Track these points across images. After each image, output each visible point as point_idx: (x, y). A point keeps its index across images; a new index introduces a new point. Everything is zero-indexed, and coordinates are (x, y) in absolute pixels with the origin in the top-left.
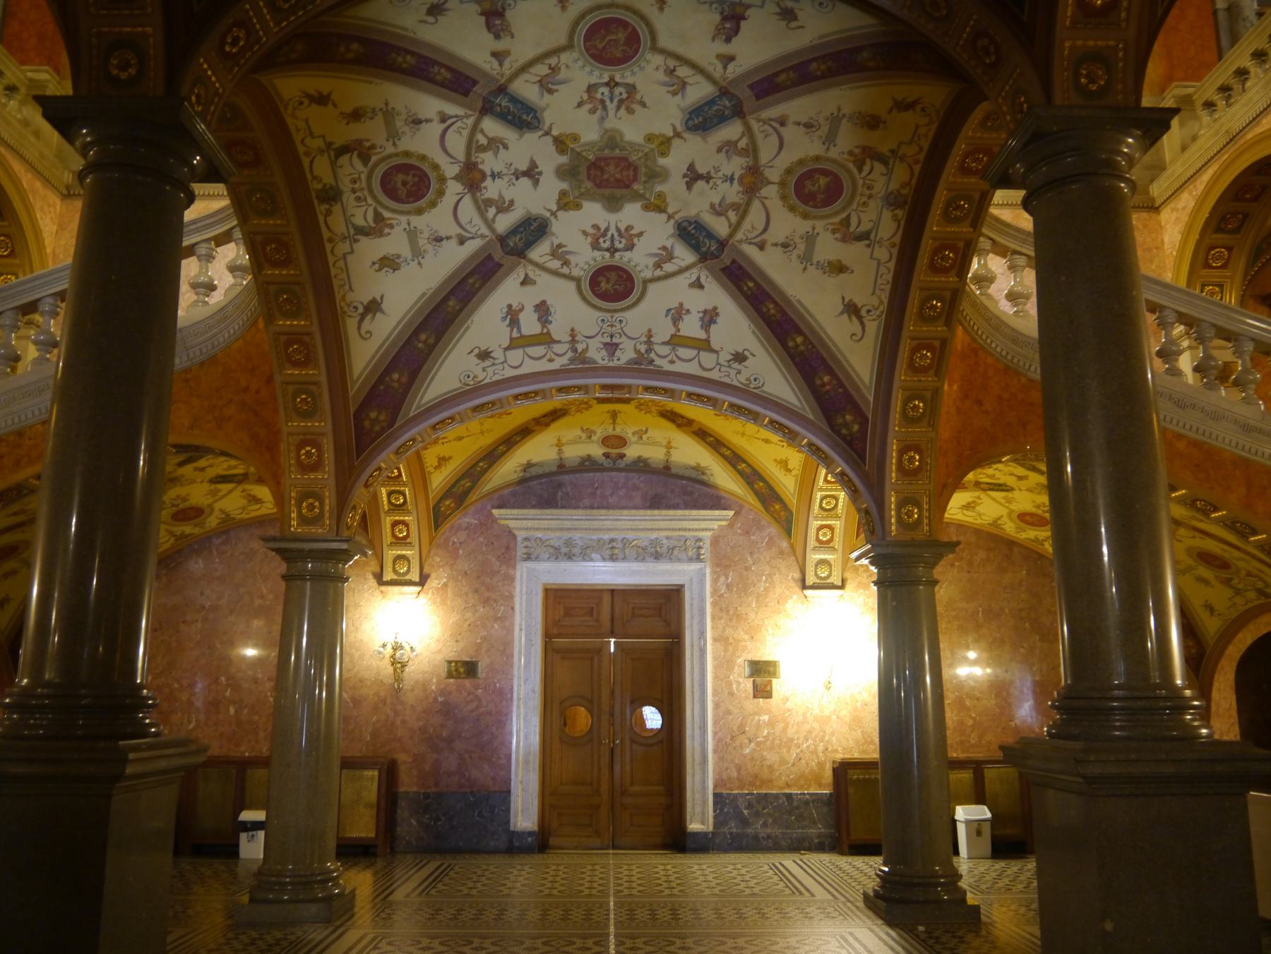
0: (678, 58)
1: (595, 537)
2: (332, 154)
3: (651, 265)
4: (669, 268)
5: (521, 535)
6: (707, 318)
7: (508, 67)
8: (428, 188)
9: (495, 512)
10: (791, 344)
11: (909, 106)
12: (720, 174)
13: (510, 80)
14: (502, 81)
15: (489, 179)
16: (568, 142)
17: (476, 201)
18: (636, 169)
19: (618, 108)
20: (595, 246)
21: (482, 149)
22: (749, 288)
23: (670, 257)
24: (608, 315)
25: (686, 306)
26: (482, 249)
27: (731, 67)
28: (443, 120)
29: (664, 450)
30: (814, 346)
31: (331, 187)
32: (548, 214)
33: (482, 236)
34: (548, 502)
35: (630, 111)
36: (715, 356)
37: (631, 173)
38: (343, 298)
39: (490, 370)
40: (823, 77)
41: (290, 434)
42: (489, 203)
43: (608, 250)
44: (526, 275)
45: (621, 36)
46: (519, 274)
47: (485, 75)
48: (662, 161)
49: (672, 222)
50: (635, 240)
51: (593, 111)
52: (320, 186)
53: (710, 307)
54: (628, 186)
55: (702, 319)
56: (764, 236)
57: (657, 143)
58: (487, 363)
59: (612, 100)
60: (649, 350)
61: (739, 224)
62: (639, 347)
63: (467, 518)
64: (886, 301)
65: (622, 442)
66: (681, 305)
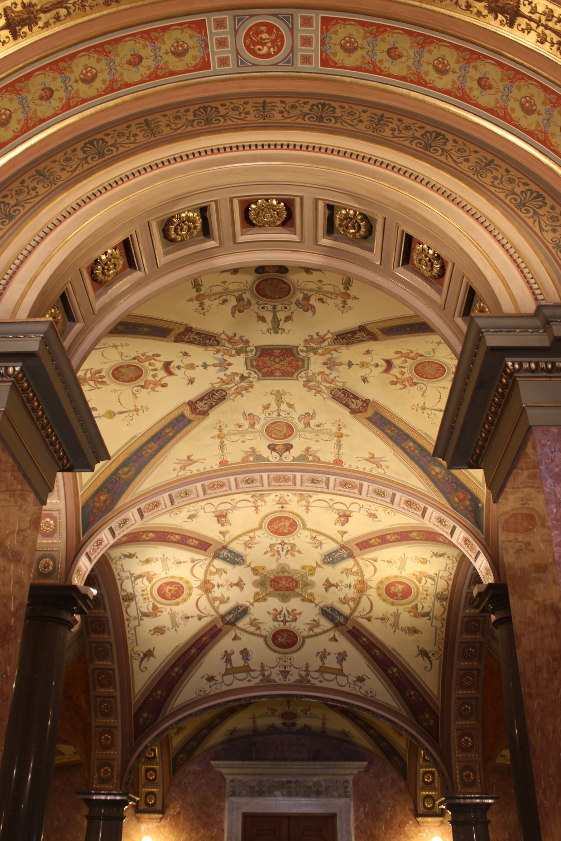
0: (317, 532)
1: (277, 779)
2: (133, 578)
3: (307, 629)
4: (317, 630)
5: (228, 778)
6: (340, 657)
7: (228, 538)
8: (183, 592)
9: (212, 762)
10: (390, 672)
11: (442, 555)
12: (343, 584)
13: (229, 543)
14: (225, 544)
15: (216, 588)
16: (260, 570)
17: (208, 598)
18: (297, 582)
19: (286, 554)
20: (275, 619)
21: (212, 574)
22: (364, 641)
23: (318, 625)
24: (283, 656)
25: (328, 651)
26: (212, 621)
27: (345, 536)
28: (193, 562)
29: (321, 721)
30: (403, 674)
31: (131, 594)
32: (248, 604)
33: (211, 615)
34: (245, 756)
35: (293, 555)
36: (346, 678)
37: (294, 584)
38: (132, 650)
39: (214, 687)
40: (394, 541)
41: (98, 727)
42: (215, 599)
43: (282, 621)
44: (236, 635)
45: (287, 523)
46: (232, 634)
47: (216, 541)
48: (311, 578)
49: (318, 607)
50: (298, 616)
51: (273, 556)
52: (125, 594)
53: (342, 651)
54: (293, 590)
55: (337, 658)
56: (371, 614)
57: (308, 569)
58: (212, 683)
59: (283, 550)
60: (307, 675)
61: (356, 608)
62: (301, 673)
63: (194, 767)
64: (442, 649)
65: (294, 716)
66: (325, 650)
